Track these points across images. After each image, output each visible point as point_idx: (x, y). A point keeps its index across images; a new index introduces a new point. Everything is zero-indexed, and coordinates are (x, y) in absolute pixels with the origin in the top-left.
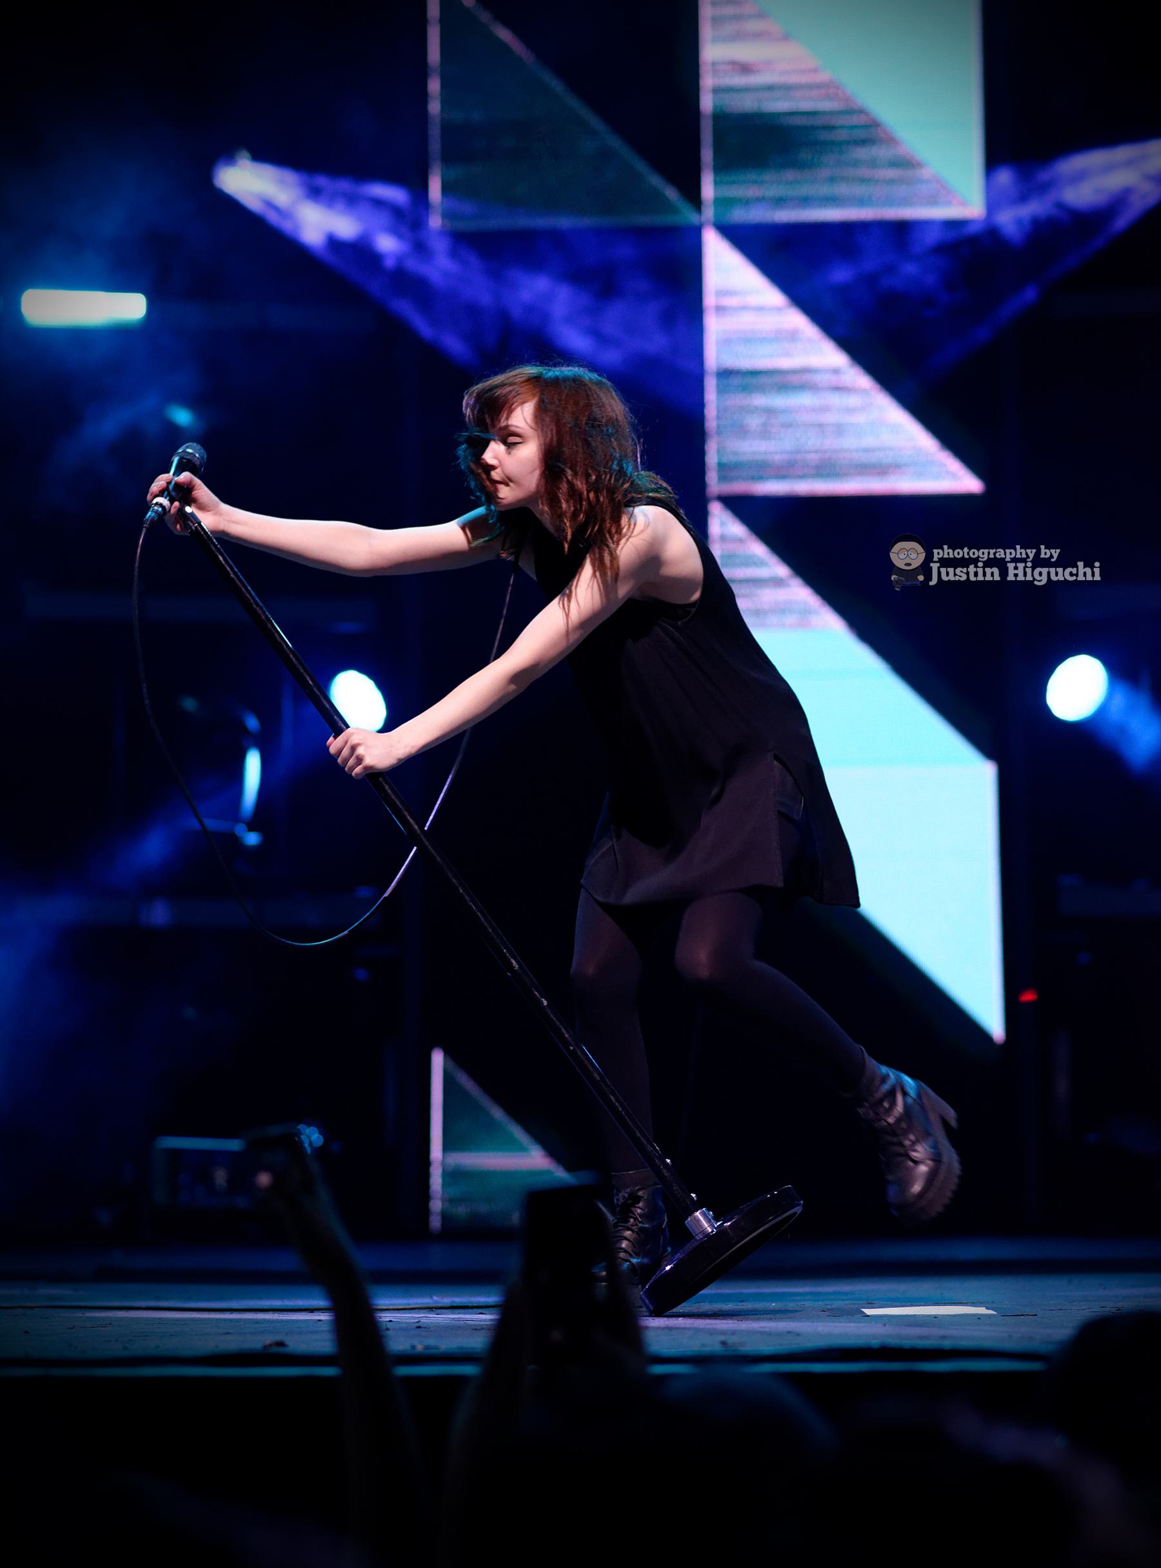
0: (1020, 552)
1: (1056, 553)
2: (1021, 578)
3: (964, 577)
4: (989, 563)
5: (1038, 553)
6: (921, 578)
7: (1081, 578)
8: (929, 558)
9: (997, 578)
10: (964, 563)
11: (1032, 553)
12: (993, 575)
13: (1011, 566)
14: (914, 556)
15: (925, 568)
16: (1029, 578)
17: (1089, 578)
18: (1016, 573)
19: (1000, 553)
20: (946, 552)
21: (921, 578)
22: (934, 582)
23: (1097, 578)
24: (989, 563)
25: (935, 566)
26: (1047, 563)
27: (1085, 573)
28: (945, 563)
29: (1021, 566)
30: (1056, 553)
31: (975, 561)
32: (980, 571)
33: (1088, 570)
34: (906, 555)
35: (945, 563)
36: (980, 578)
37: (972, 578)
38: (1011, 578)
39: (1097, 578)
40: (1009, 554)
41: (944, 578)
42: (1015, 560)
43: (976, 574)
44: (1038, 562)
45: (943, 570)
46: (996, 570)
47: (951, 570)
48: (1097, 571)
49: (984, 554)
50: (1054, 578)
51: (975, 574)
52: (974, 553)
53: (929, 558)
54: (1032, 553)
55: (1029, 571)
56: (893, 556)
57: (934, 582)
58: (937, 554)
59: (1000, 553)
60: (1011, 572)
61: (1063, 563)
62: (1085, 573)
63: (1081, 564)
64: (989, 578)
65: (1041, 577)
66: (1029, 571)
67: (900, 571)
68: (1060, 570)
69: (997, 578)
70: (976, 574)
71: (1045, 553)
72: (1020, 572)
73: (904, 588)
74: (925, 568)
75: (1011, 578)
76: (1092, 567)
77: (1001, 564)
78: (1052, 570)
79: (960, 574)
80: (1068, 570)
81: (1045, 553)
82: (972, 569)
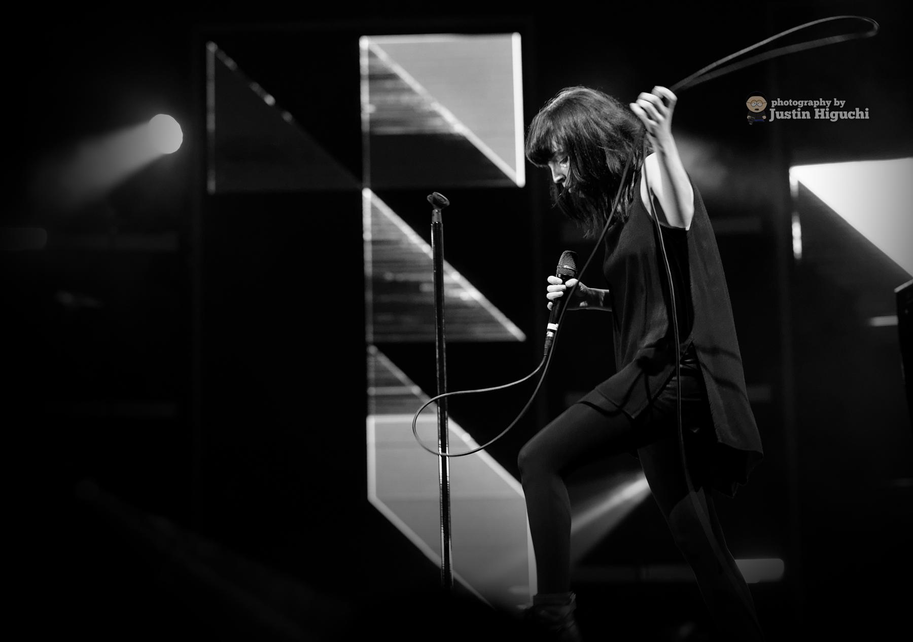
0: (822, 102)
1: (843, 103)
2: (823, 117)
3: (789, 117)
4: (805, 109)
5: (833, 103)
6: (764, 117)
7: (858, 117)
8: (769, 106)
9: (809, 117)
10: (789, 108)
11: (829, 103)
12: (807, 115)
13: (817, 110)
14: (760, 104)
15: (767, 111)
16: (827, 117)
17: (862, 117)
18: (819, 114)
19: (811, 103)
20: (779, 102)
21: (764, 117)
22: (772, 120)
23: (867, 117)
24: (805, 109)
25: (772, 110)
26: (838, 109)
27: (860, 114)
28: (778, 108)
29: (823, 110)
30: (843, 103)
31: (796, 108)
32: (799, 113)
33: (862, 113)
34: (756, 104)
35: (778, 108)
36: (799, 117)
37: (794, 117)
38: (817, 117)
39: (867, 117)
40: (816, 103)
41: (778, 117)
42: (819, 107)
43: (796, 115)
44: (833, 108)
45: (777, 113)
46: (808, 113)
47: (782, 113)
48: (867, 113)
49: (801, 103)
50: (842, 117)
51: (796, 115)
52: (795, 103)
53: (769, 106)
54: (829, 103)
55: (827, 113)
56: (748, 105)
57: (772, 120)
58: (774, 103)
59: (811, 103)
60: (817, 114)
61: (847, 108)
62: (860, 114)
63: (857, 109)
64: (804, 117)
65: (834, 117)
66: (827, 113)
67: (752, 113)
68: (845, 113)
69: (809, 117)
70: (796, 115)
71: (837, 103)
72: (822, 114)
73: (754, 123)
74: (767, 111)
75: (817, 117)
76: (864, 111)
77: (811, 109)
78: (841, 113)
79: (787, 115)
80: (850, 113)
81: (837, 103)
82: (794, 112)
